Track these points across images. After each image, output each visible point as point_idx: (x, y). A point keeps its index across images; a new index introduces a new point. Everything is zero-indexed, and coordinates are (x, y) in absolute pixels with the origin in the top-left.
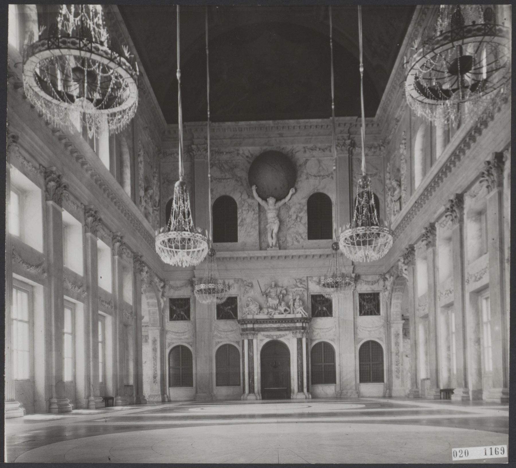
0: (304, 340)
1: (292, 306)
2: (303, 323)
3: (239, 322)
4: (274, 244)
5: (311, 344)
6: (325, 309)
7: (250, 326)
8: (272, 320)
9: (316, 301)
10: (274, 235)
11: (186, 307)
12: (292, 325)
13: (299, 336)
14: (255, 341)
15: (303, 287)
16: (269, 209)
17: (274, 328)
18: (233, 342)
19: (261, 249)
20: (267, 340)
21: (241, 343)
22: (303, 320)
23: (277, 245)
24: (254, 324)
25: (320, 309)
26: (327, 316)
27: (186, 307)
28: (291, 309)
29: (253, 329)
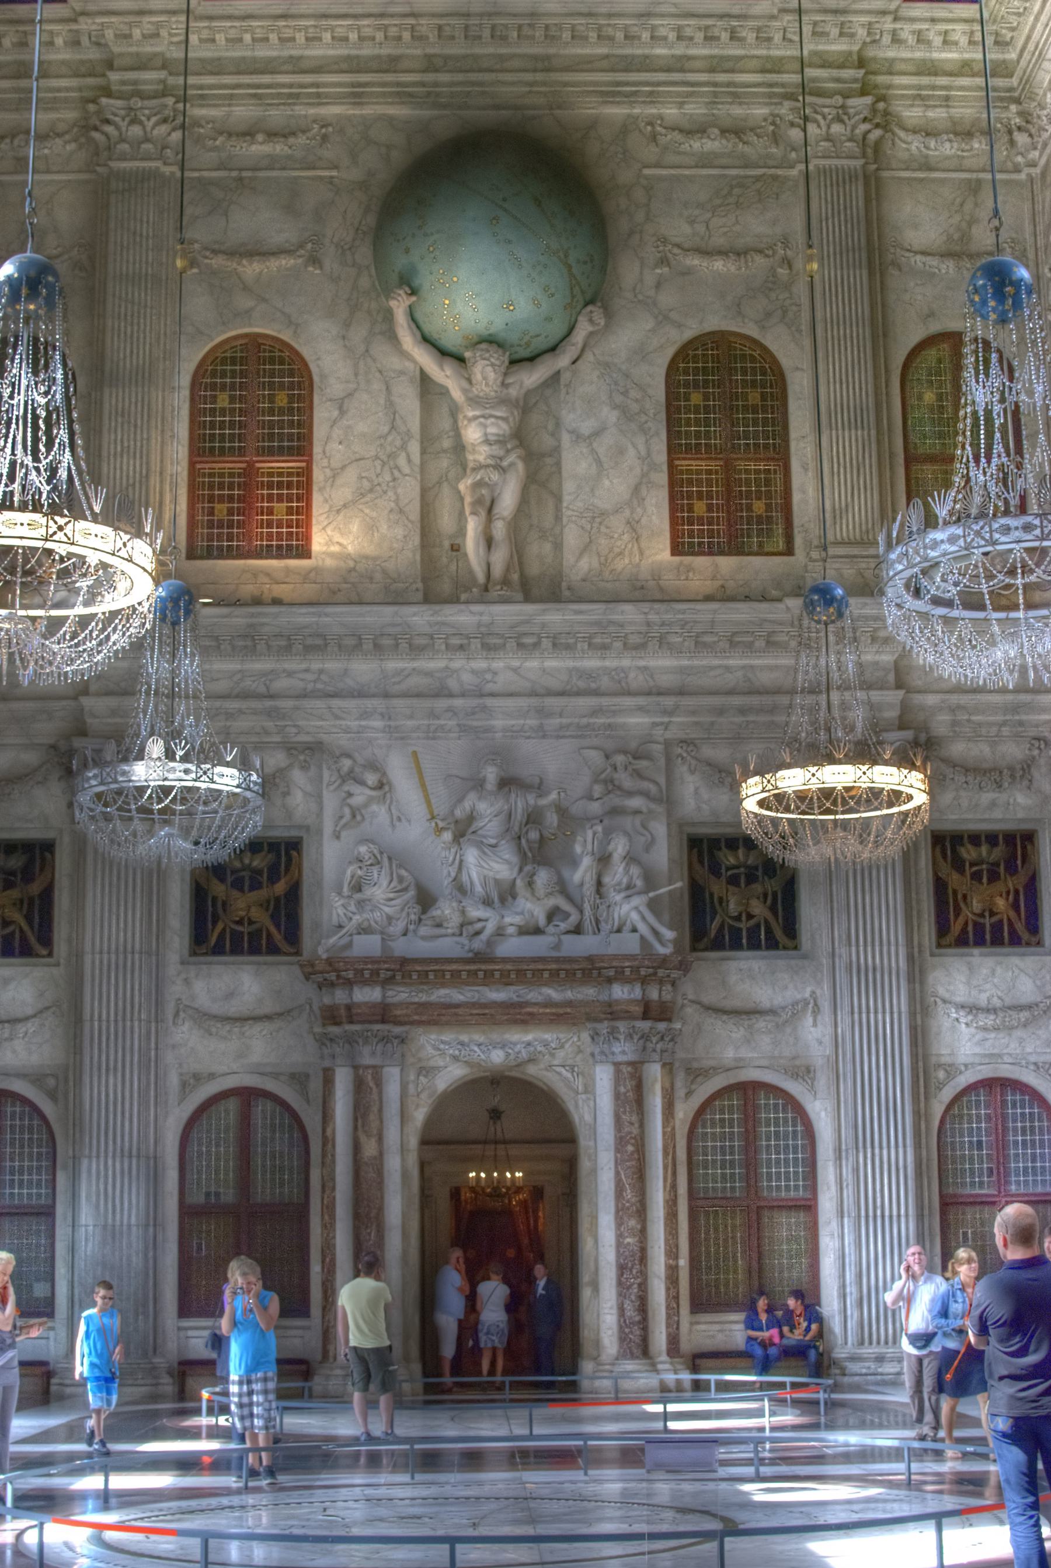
0: (654, 1072)
1: (589, 890)
2: (644, 981)
3: (309, 970)
4: (497, 571)
5: (689, 1094)
6: (758, 908)
7: (367, 995)
8: (481, 966)
9: (715, 870)
10: (499, 529)
11: (35, 889)
12: (588, 992)
13: (624, 1050)
14: (392, 1076)
15: (646, 794)
16: (474, 401)
18: (276, 1076)
19: (429, 598)
20: (450, 1075)
21: (315, 1085)
22: (646, 969)
23: (515, 577)
24: (389, 981)
25: (733, 907)
26: (773, 944)
27: (35, 889)
28: (587, 907)
29: (383, 1014)
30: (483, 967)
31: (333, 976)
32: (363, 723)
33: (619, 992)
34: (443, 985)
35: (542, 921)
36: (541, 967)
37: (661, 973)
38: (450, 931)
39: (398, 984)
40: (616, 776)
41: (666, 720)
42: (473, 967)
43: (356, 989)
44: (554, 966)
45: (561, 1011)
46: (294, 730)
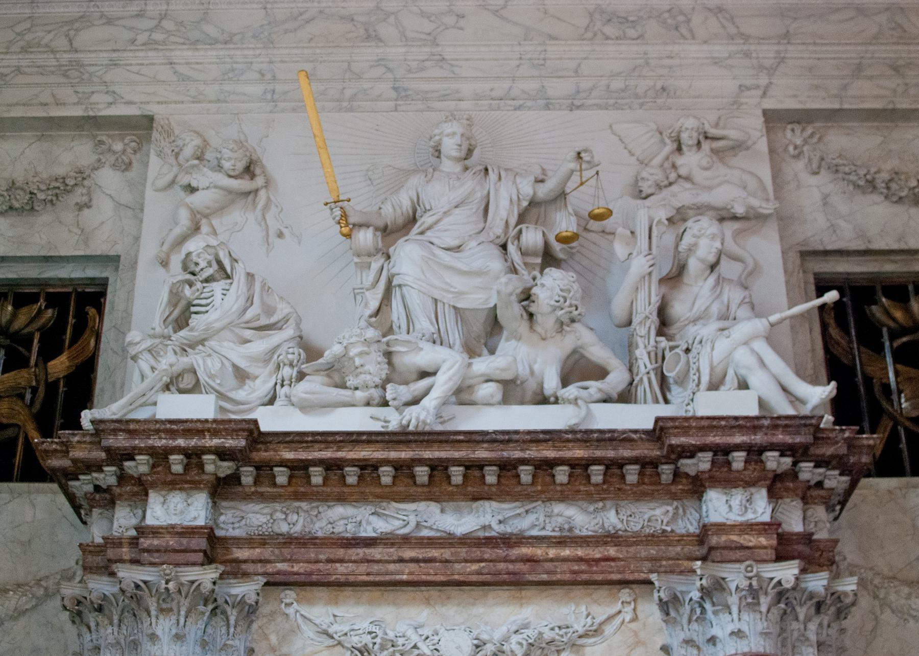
12: (654, 515)
17: (449, 540)
30: (427, 454)
31: (108, 477)
32: (228, 87)
33: (721, 506)
34: (341, 499)
35: (551, 383)
36: (551, 454)
37: (807, 471)
38: (360, 395)
39: (247, 497)
40: (680, 161)
41: (763, 81)
42: (404, 454)
43: (154, 498)
44: (579, 453)
45: (597, 553)
46: (109, 99)
